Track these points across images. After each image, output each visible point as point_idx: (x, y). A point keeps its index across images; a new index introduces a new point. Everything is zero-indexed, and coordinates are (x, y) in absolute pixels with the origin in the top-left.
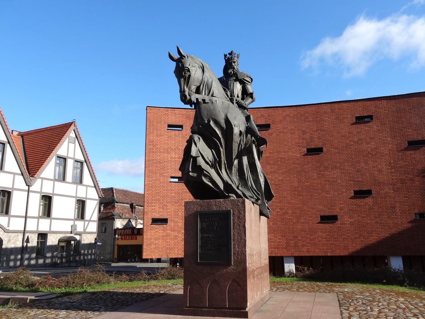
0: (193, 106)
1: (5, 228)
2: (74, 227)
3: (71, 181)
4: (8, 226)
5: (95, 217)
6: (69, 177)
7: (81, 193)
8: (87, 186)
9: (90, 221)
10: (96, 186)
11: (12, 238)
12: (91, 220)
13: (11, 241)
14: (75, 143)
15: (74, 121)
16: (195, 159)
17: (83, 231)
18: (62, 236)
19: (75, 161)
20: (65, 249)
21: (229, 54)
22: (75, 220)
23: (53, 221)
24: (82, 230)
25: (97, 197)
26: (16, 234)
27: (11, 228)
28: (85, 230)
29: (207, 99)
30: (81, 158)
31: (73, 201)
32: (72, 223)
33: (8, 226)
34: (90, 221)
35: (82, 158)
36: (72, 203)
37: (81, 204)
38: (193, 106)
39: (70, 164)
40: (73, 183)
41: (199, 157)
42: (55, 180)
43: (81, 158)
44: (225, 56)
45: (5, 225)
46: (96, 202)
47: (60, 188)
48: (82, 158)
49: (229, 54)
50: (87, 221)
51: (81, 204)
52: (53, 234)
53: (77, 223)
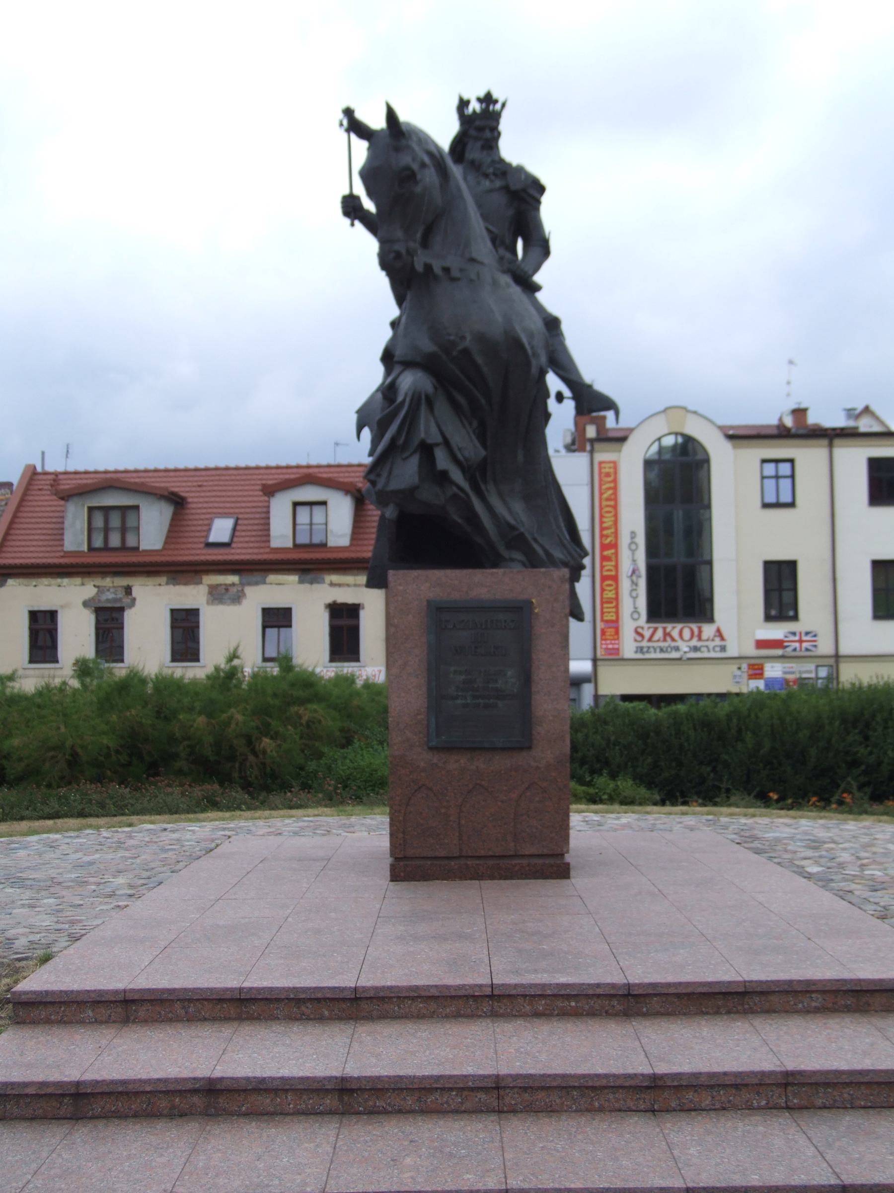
16: (426, 450)
21: (479, 100)
29: (454, 262)
41: (437, 445)
44: (463, 104)
49: (479, 100)
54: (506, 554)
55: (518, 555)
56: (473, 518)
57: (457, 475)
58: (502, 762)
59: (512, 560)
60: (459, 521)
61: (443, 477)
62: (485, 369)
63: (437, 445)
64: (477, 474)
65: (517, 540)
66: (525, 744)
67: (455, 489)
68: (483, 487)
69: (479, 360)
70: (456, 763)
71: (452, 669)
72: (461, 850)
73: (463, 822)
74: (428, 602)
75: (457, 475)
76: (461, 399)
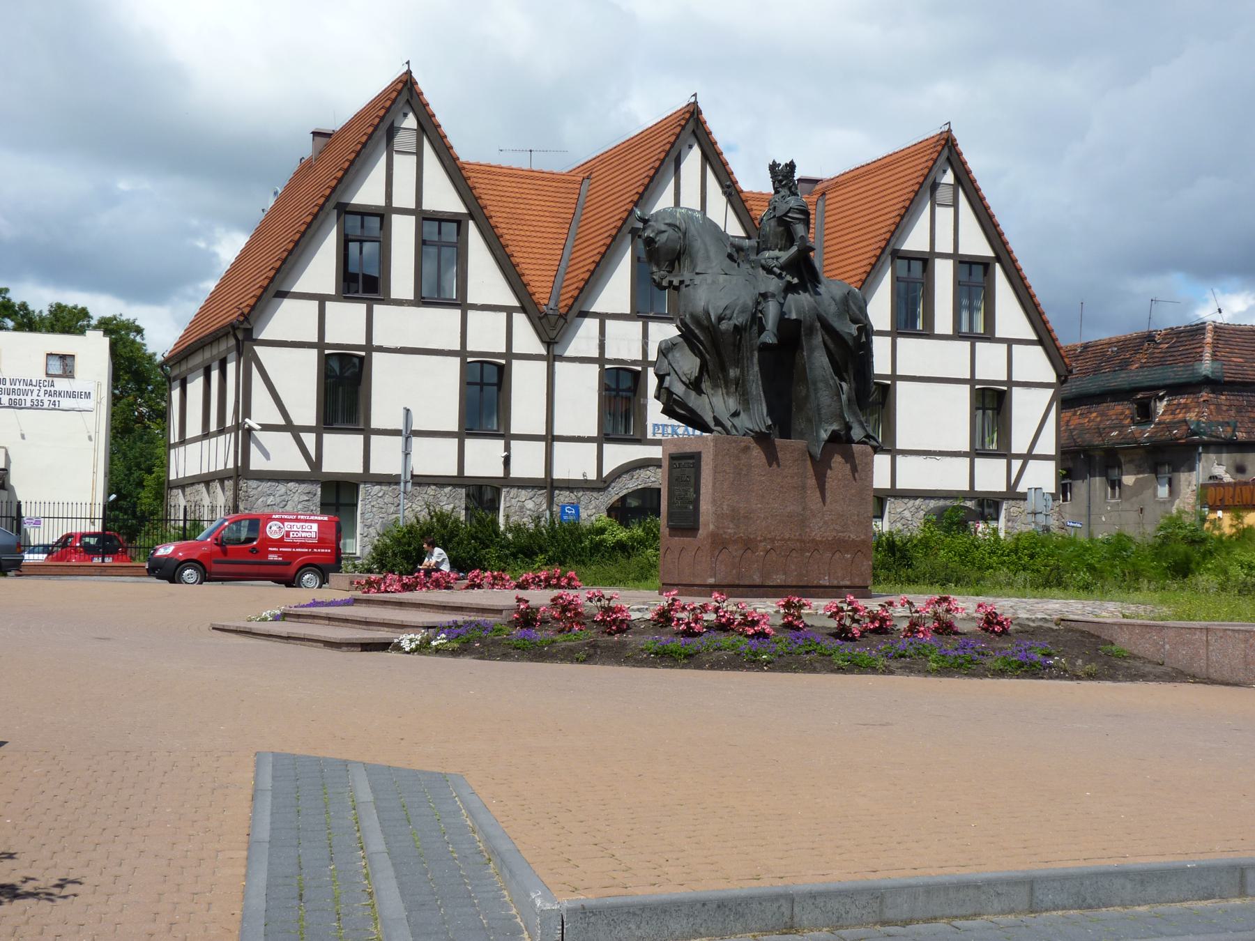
3: (950, 332)
5: (1048, 444)
6: (943, 320)
8: (1010, 342)
9: (1028, 457)
10: (1045, 338)
12: (1035, 452)
14: (955, 205)
15: (946, 128)
17: (1004, 489)
19: (961, 262)
23: (900, 459)
24: (1001, 487)
25: (1051, 377)
28: (1012, 487)
30: (976, 244)
34: (1028, 457)
35: (985, 250)
37: (992, 403)
39: (944, 273)
40: (957, 335)
43: (976, 244)
46: (1050, 392)
48: (985, 250)
50: (1018, 456)
51: (992, 403)
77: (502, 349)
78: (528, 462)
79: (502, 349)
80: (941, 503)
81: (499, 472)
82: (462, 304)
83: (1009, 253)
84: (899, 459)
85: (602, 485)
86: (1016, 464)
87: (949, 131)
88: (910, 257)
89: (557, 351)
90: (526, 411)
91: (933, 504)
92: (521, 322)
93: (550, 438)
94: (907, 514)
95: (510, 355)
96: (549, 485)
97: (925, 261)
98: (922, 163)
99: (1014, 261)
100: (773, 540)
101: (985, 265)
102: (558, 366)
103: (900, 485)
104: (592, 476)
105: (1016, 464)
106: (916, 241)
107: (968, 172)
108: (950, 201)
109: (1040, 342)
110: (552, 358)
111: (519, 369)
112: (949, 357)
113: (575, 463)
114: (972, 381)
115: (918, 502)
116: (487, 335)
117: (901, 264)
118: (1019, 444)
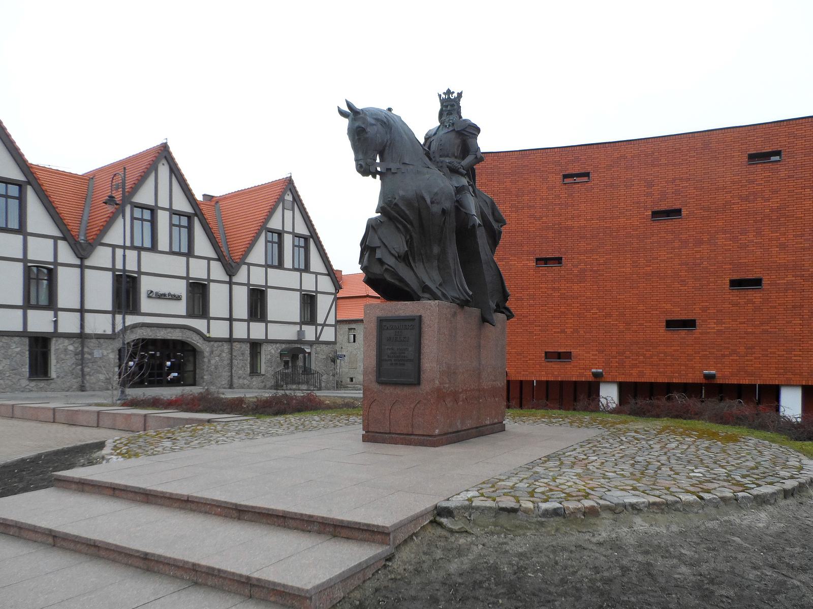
0: (378, 177)
1: (203, 334)
2: (301, 333)
4: (209, 332)
7: (309, 283)
8: (317, 274)
11: (215, 349)
13: (214, 353)
14: (293, 210)
18: (284, 346)
20: (290, 365)
22: (302, 323)
23: (269, 324)
26: (220, 343)
27: (214, 334)
28: (317, 338)
30: (302, 229)
31: (297, 295)
32: (297, 328)
33: (209, 332)
35: (306, 232)
36: (295, 300)
37: (309, 301)
38: (378, 177)
39: (288, 240)
40: (294, 269)
42: (267, 266)
43: (302, 229)
45: (205, 331)
47: (276, 277)
48: (306, 232)
50: (320, 325)
51: (309, 301)
52: (272, 344)
53: (304, 327)
54: (421, 295)
55: (427, 295)
56: (401, 280)
57: (390, 261)
58: (407, 390)
59: (423, 297)
60: (393, 281)
61: (381, 261)
62: (407, 212)
63: (379, 247)
64: (404, 259)
65: (426, 289)
66: (418, 383)
67: (386, 266)
68: (413, 265)
69: (403, 208)
70: (389, 390)
71: (387, 347)
72: (390, 430)
73: (391, 417)
74: (378, 317)
75: (390, 261)
76: (400, 227)
77: (51, 259)
78: (69, 324)
79: (51, 259)
80: (288, 346)
81: (51, 330)
82: (21, 230)
83: (316, 234)
84: (269, 324)
85: (113, 337)
86: (319, 328)
87: (291, 177)
88: (272, 231)
89: (88, 263)
90: (67, 295)
91: (284, 346)
92: (63, 246)
93: (82, 311)
94: (273, 351)
95: (56, 263)
96: (82, 337)
97: (280, 234)
98: (278, 190)
99: (318, 238)
100: (466, 390)
101: (306, 239)
102: (88, 272)
103: (269, 338)
104: (109, 331)
105: (319, 328)
106: (275, 223)
107: (299, 196)
108: (290, 207)
109: (329, 275)
110: (82, 267)
111: (62, 272)
112: (290, 279)
113: (99, 324)
114: (300, 290)
115: (278, 345)
116: (41, 251)
117: (269, 234)
118: (320, 319)
